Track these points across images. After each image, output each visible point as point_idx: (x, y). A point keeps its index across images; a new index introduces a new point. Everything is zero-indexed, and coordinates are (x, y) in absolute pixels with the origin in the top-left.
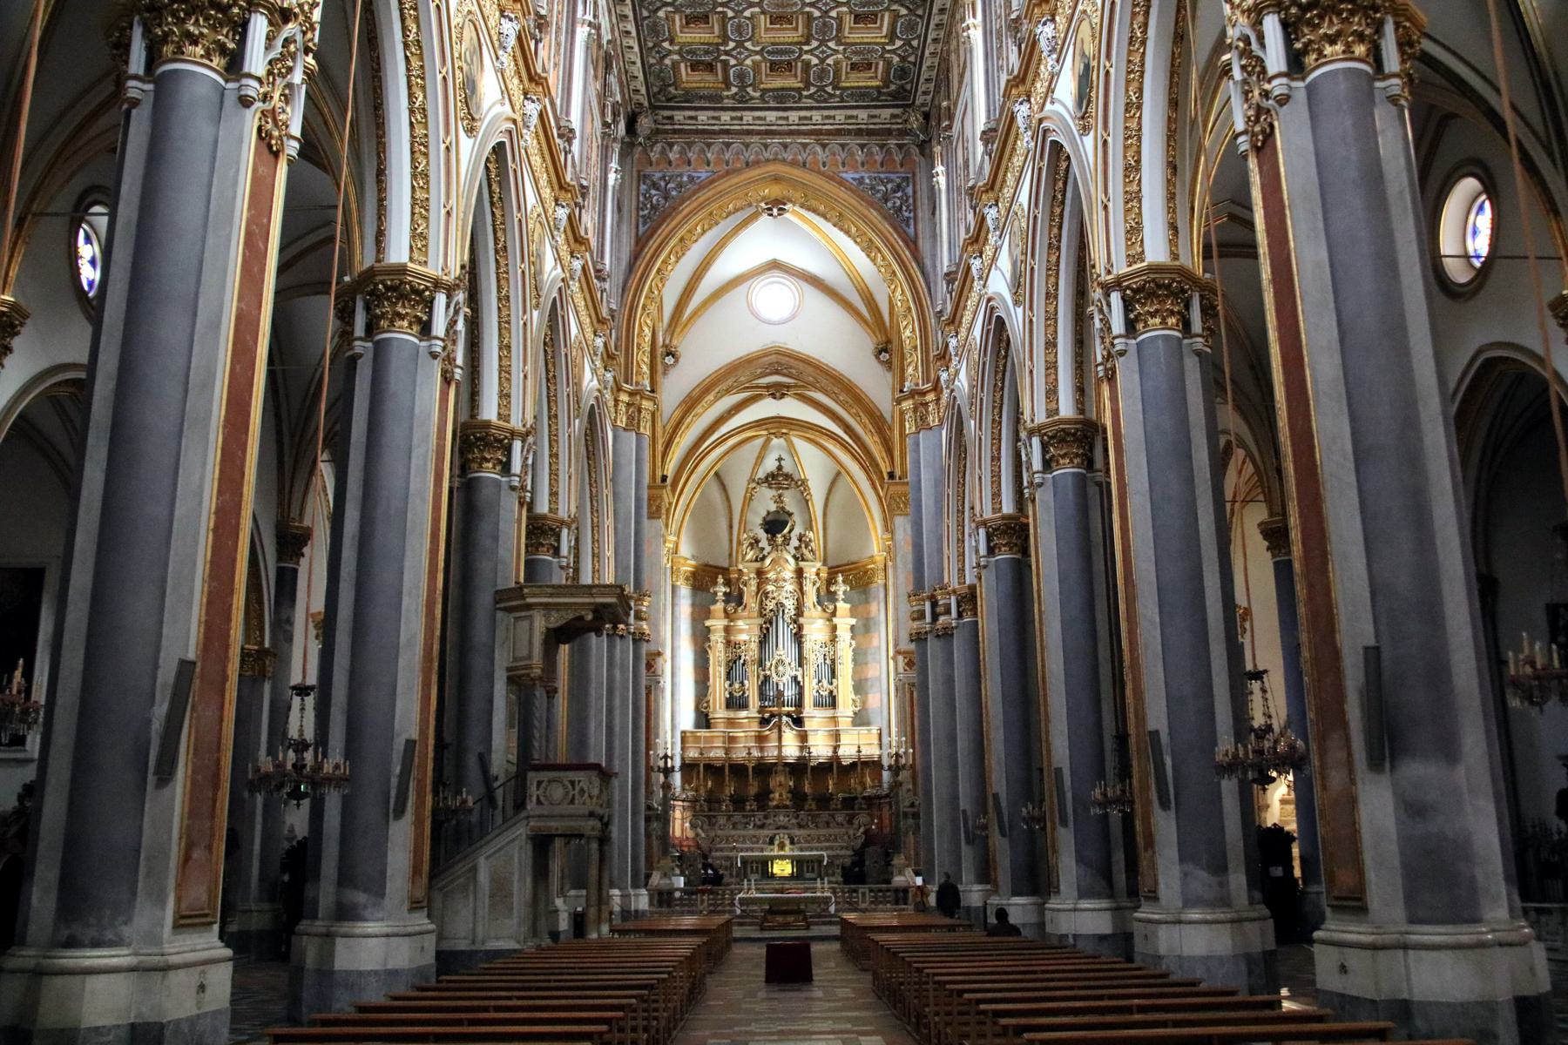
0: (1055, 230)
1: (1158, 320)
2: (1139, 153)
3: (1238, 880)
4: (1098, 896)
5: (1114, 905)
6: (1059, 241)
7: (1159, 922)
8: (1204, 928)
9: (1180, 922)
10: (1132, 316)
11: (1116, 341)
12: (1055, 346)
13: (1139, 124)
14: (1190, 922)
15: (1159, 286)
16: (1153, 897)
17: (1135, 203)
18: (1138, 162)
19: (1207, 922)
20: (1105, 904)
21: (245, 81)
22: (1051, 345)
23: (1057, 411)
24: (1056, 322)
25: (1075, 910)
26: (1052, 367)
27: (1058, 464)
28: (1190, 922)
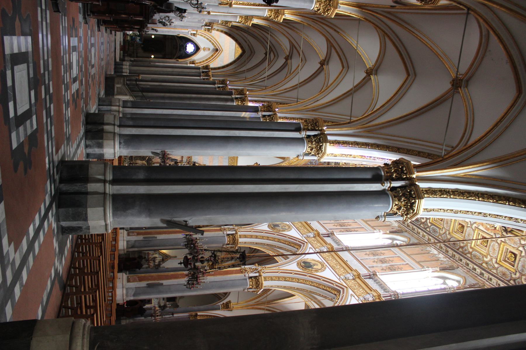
0: (282, 242)
1: (251, 284)
2: (288, 281)
3: (132, 298)
4: (127, 246)
5: (125, 249)
6: (280, 242)
7: (123, 284)
8: (122, 293)
9: (123, 288)
10: (253, 278)
11: (248, 275)
12: (256, 238)
13: (294, 282)
14: (123, 291)
15: (258, 285)
16: (129, 281)
17: (277, 279)
18: (286, 281)
19: (123, 294)
20: (125, 247)
21: (302, 157)
22: (257, 237)
23: (240, 238)
24: (262, 239)
25: (124, 240)
26: (251, 237)
27: (228, 238)
28: (123, 291)
